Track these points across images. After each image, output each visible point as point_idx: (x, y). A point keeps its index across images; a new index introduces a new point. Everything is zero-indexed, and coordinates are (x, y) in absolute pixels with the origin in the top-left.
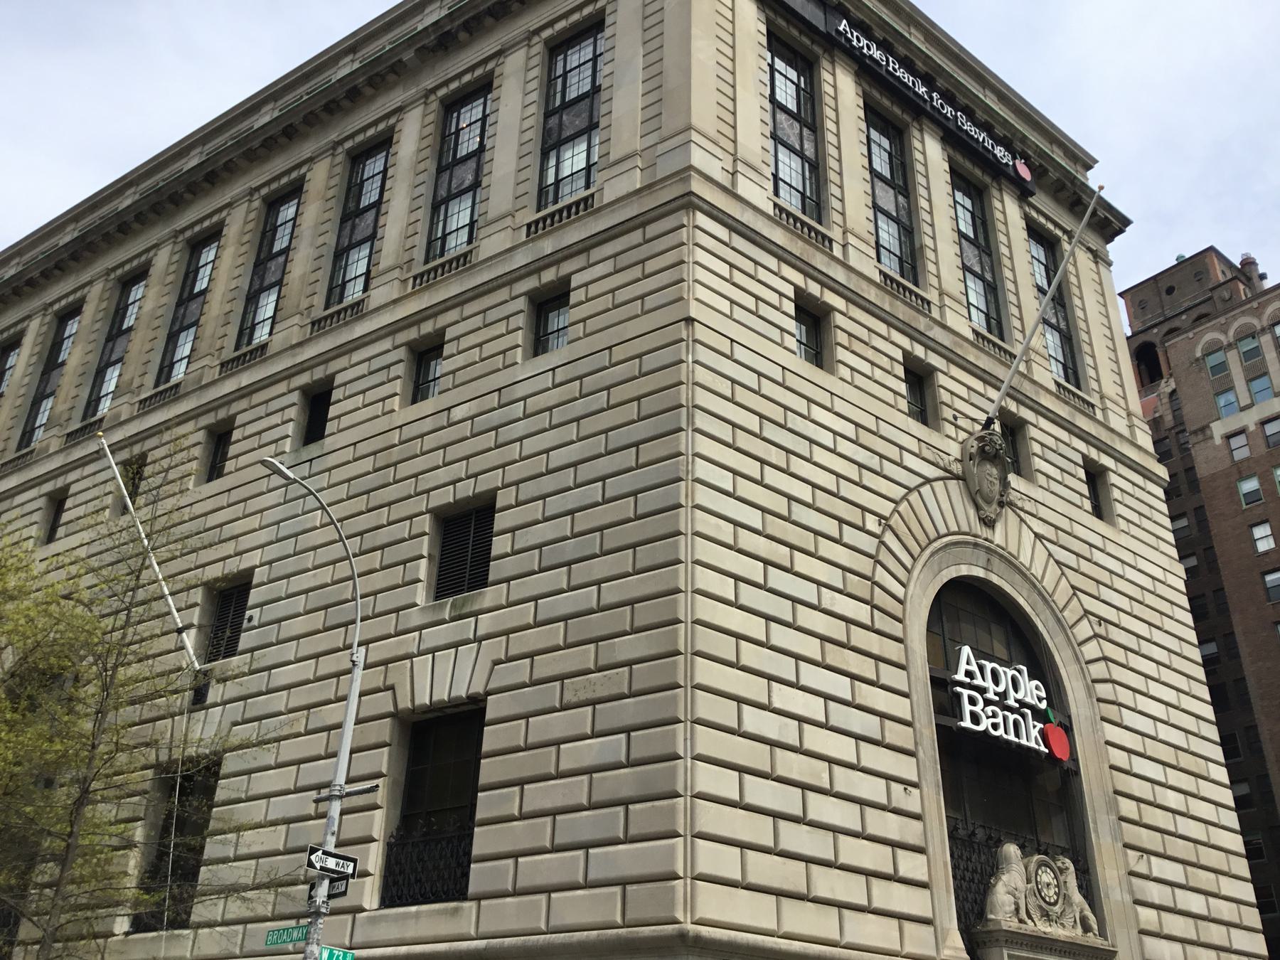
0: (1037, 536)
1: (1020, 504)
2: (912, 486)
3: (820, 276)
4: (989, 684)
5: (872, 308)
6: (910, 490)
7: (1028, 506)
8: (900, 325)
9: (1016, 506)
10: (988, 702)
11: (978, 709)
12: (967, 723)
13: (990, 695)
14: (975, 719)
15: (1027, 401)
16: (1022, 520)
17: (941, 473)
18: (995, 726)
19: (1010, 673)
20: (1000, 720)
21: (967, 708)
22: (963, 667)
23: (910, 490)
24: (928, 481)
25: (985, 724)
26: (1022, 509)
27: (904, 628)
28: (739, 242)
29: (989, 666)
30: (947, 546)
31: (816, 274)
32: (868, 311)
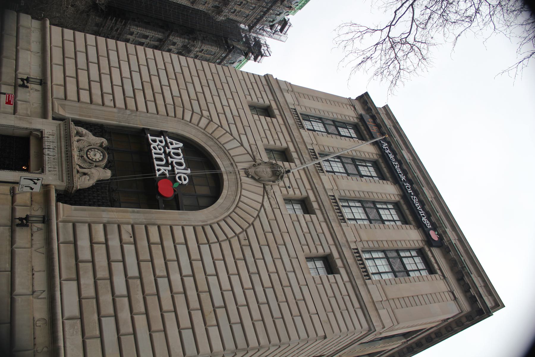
0: (263, 205)
1: (270, 197)
2: (234, 135)
3: (283, 114)
4: (173, 151)
5: (291, 134)
6: (232, 135)
7: (273, 202)
8: (296, 147)
9: (267, 194)
10: (164, 147)
11: (158, 142)
12: (150, 138)
13: (168, 150)
14: (155, 141)
15: (325, 215)
16: (263, 196)
17: (251, 153)
18: (155, 148)
19: (183, 161)
20: (158, 151)
21: (158, 139)
22: (174, 142)
23: (232, 135)
24: (242, 145)
25: (154, 145)
26: (269, 199)
27: (172, 117)
28: (267, 88)
29: (180, 151)
30: (221, 147)
31: (282, 113)
32: (289, 134)
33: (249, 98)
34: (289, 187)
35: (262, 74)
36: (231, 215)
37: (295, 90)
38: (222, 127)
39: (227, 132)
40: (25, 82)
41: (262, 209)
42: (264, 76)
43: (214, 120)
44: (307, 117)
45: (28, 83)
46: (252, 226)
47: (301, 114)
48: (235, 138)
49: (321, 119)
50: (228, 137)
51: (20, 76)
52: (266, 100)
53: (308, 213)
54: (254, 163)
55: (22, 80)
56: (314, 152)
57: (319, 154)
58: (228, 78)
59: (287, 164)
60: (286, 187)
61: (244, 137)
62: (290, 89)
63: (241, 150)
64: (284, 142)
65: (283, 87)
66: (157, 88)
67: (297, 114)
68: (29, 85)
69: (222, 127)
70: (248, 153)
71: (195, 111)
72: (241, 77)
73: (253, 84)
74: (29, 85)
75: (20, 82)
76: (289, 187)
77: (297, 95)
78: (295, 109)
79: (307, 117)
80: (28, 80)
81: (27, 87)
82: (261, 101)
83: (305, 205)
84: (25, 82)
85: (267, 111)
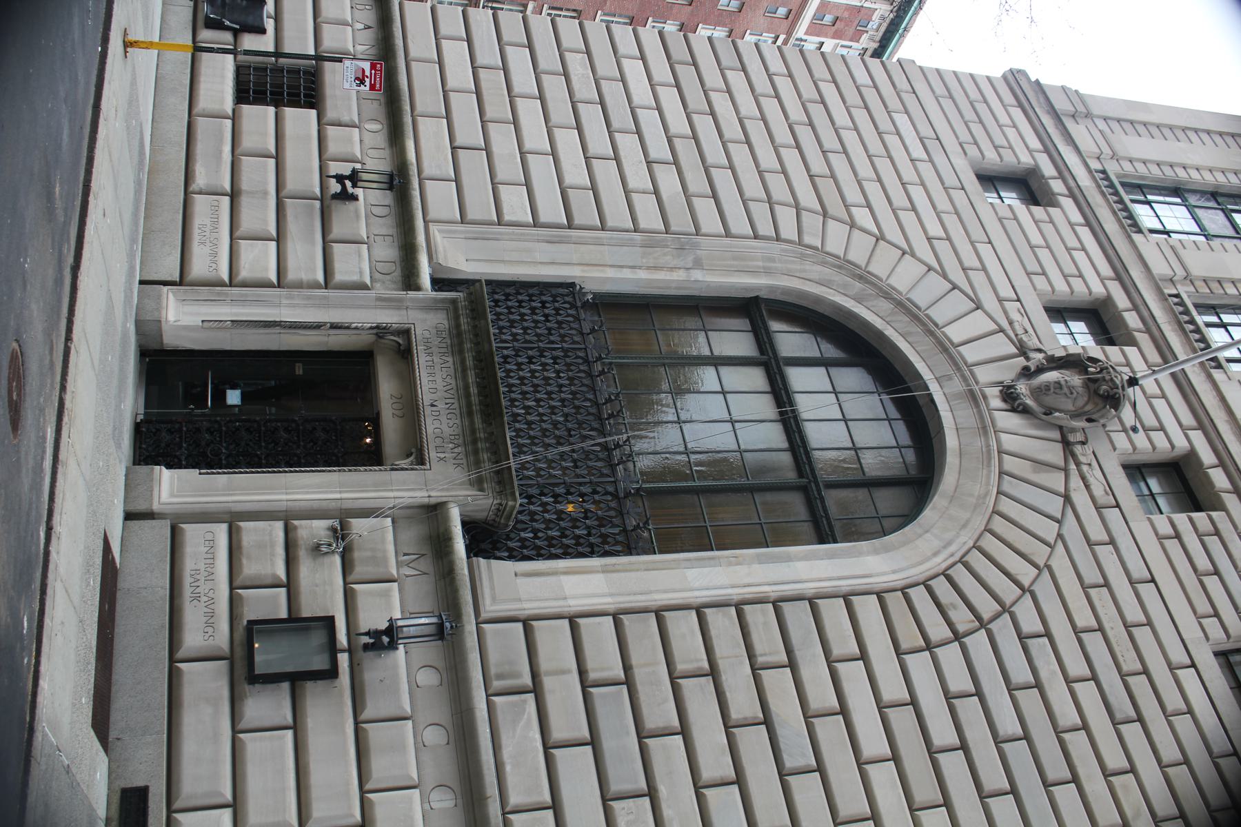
0: (1067, 499)
2: (951, 277)
6: (945, 276)
23: (945, 276)
33: (972, 151)
34: (1134, 429)
35: (997, 73)
36: (981, 543)
37: (1096, 111)
38: (913, 255)
39: (930, 269)
40: (348, 184)
41: (1069, 511)
42: (1004, 77)
43: (888, 236)
44: (1142, 189)
45: (354, 186)
46: (1046, 574)
47: (1123, 184)
48: (955, 287)
49: (1177, 191)
50: (936, 284)
51: (335, 168)
52: (1023, 152)
53: (1199, 509)
54: (1021, 361)
55: (340, 179)
56: (1182, 304)
57: (1196, 306)
58: (903, 95)
59: (1114, 352)
60: (1125, 430)
61: (978, 278)
62: (1081, 108)
63: (978, 323)
64: (1094, 281)
65: (1061, 104)
66: (715, 153)
67: (1112, 186)
68: (359, 192)
69: (913, 255)
70: (1002, 330)
71: (831, 211)
72: (940, 89)
73: (977, 105)
74: (359, 192)
75: (335, 187)
76: (1134, 429)
77: (1101, 124)
78: (1104, 172)
79: (1142, 189)
80: (354, 177)
81: (354, 198)
82: (1009, 158)
83: (1181, 482)
84: (348, 184)
85: (1030, 187)
